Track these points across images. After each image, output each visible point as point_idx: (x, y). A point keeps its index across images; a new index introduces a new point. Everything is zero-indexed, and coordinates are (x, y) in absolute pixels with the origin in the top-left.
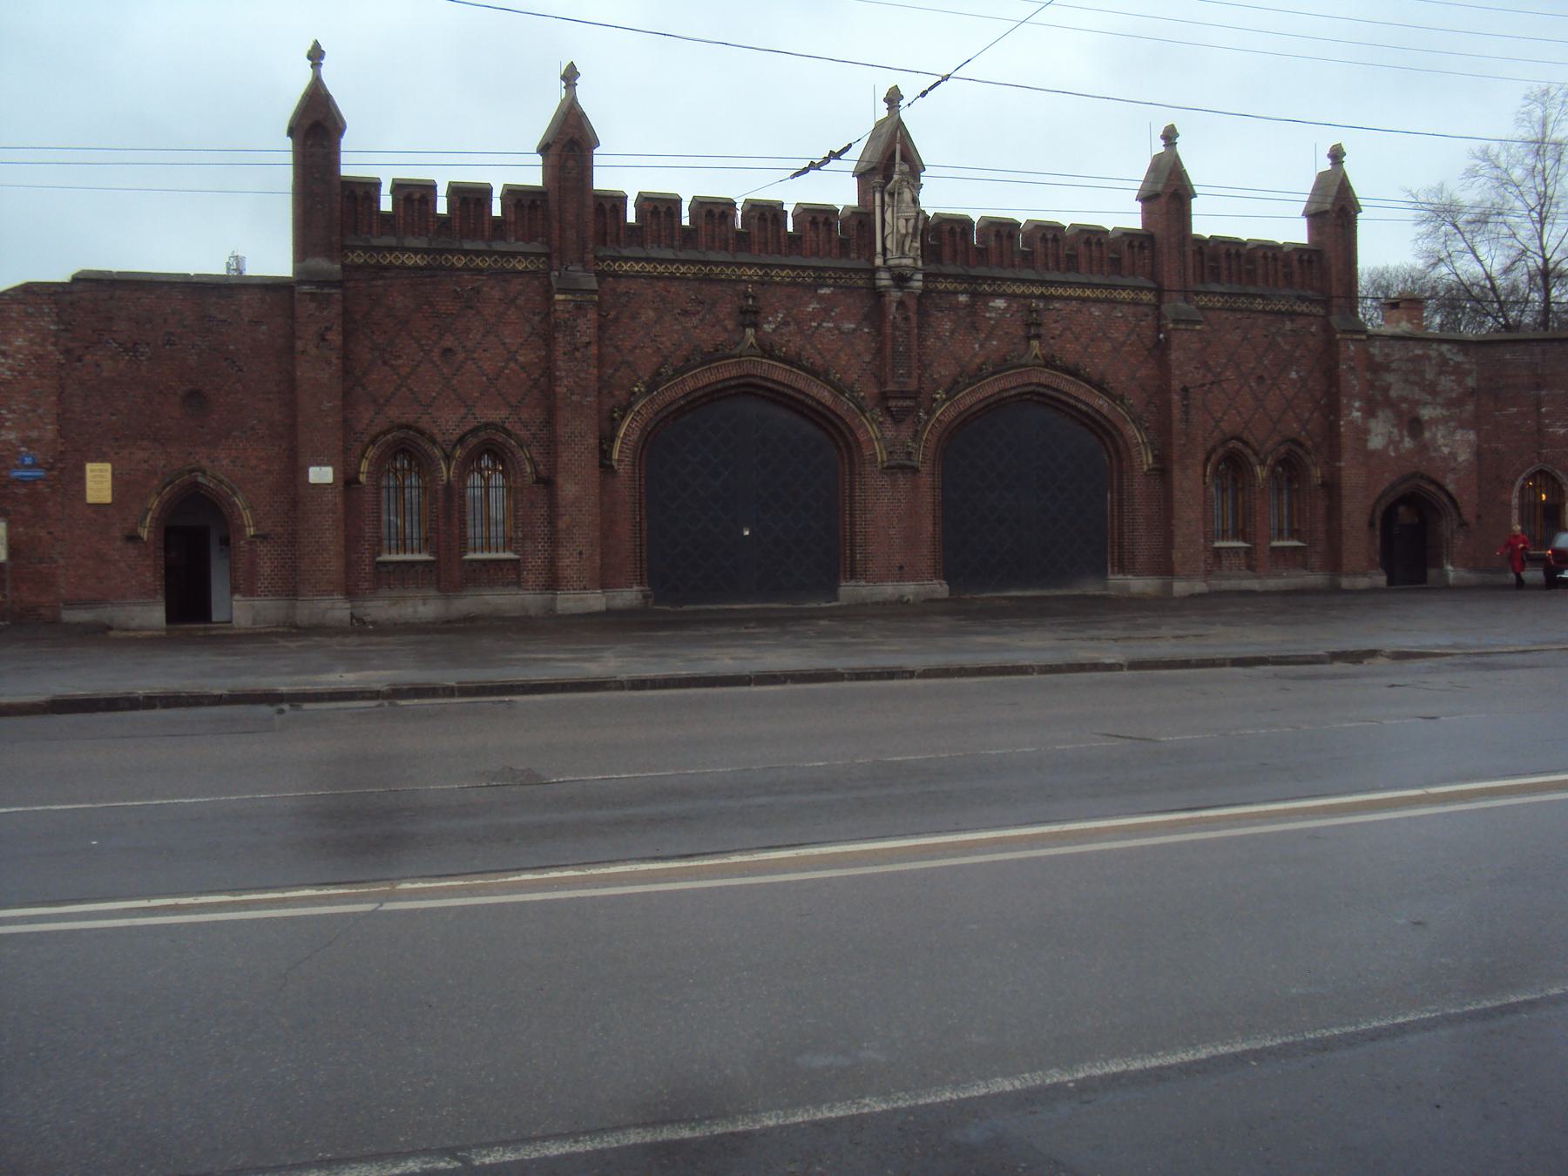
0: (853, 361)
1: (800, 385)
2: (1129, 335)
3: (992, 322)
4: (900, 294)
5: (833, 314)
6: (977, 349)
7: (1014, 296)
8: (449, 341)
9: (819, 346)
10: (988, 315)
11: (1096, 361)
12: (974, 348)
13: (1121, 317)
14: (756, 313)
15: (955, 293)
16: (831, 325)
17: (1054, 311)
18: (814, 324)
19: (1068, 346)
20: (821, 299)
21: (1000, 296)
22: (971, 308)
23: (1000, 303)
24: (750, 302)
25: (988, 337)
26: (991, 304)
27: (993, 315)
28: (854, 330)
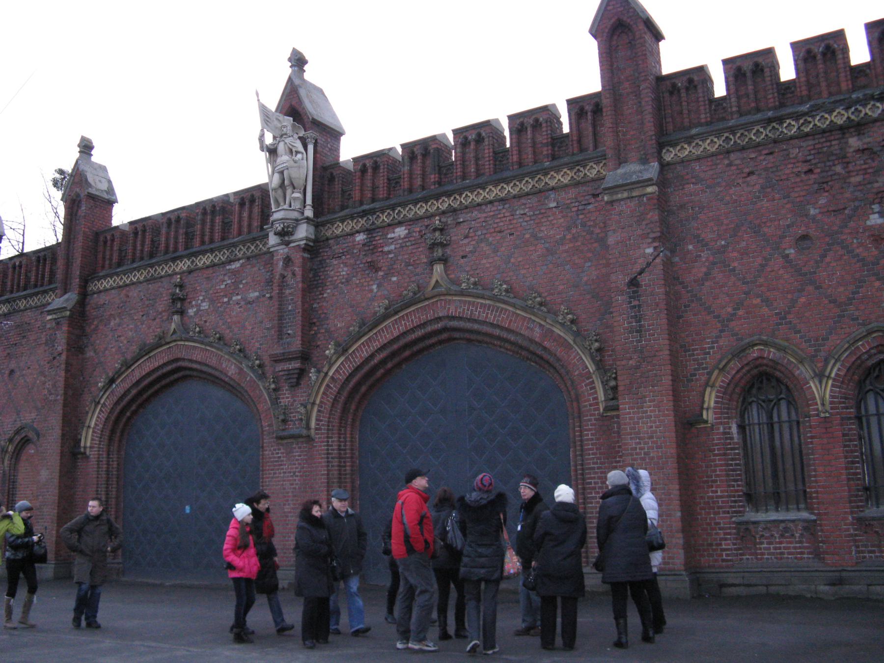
0: (256, 330)
1: (213, 362)
2: (568, 229)
3: (391, 256)
4: (286, 250)
5: (241, 286)
6: (375, 291)
7: (417, 219)
8: (13, 365)
9: (229, 320)
10: (386, 249)
11: (523, 272)
12: (371, 291)
13: (555, 207)
14: (182, 300)
15: (352, 234)
16: (239, 297)
17: (465, 224)
18: (226, 300)
19: (484, 261)
20: (234, 273)
21: (400, 224)
22: (371, 247)
23: (401, 231)
24: (177, 291)
25: (387, 275)
26: (389, 236)
27: (392, 247)
28: (257, 298)
